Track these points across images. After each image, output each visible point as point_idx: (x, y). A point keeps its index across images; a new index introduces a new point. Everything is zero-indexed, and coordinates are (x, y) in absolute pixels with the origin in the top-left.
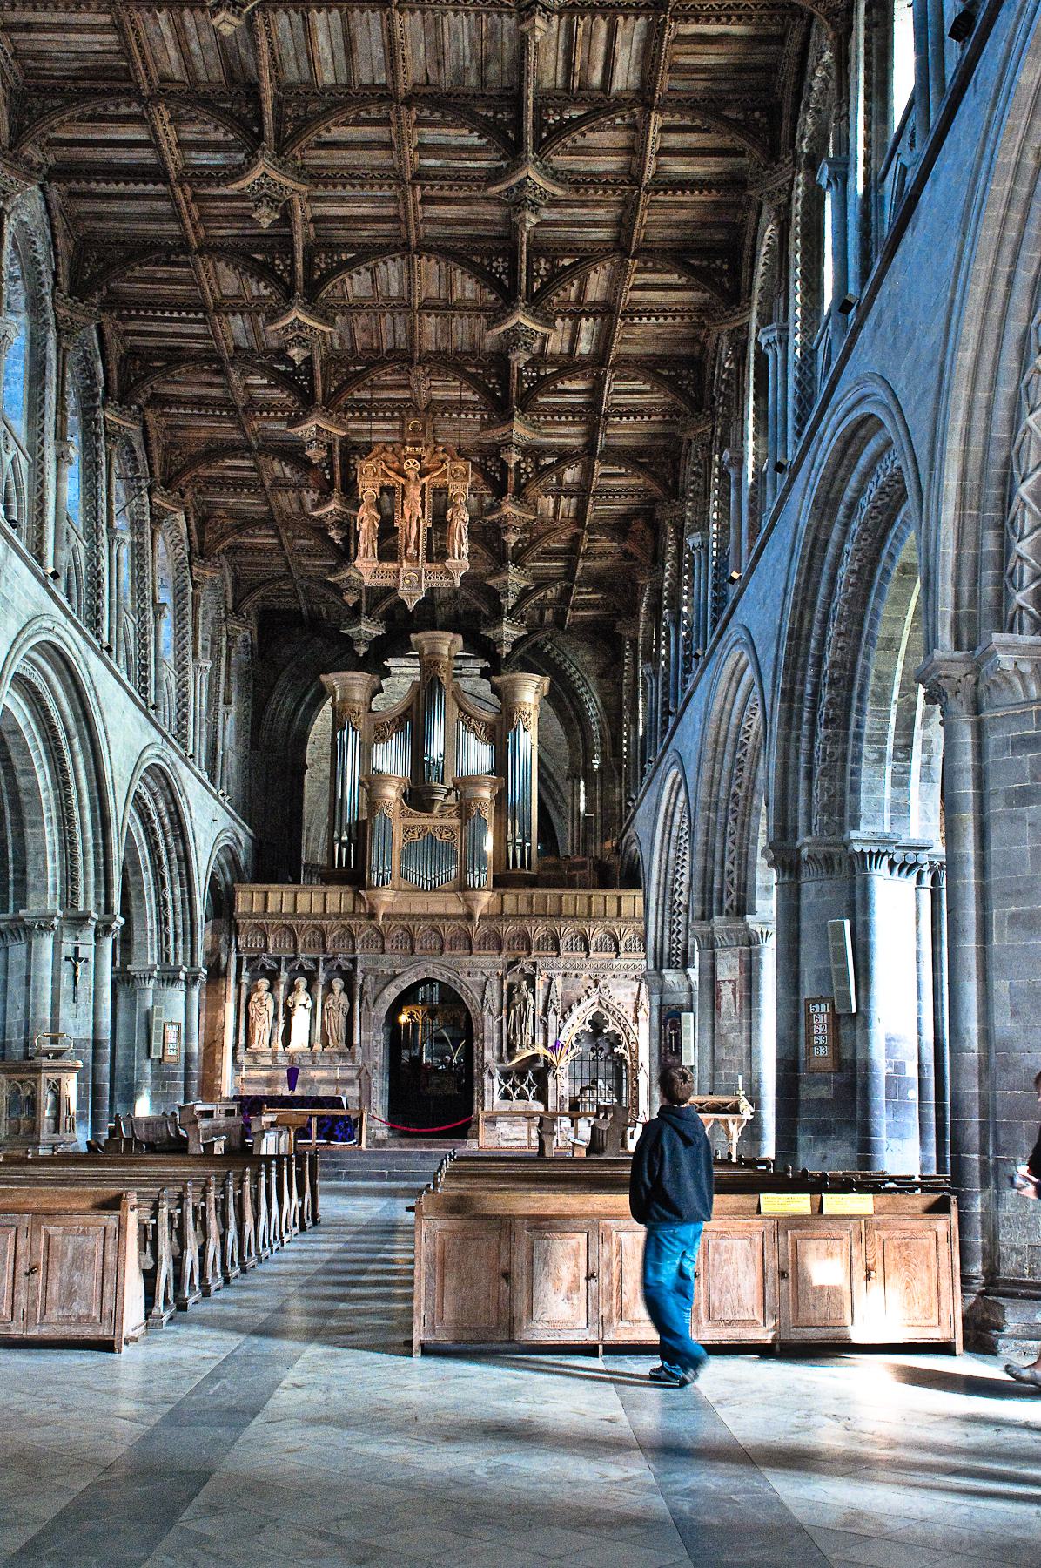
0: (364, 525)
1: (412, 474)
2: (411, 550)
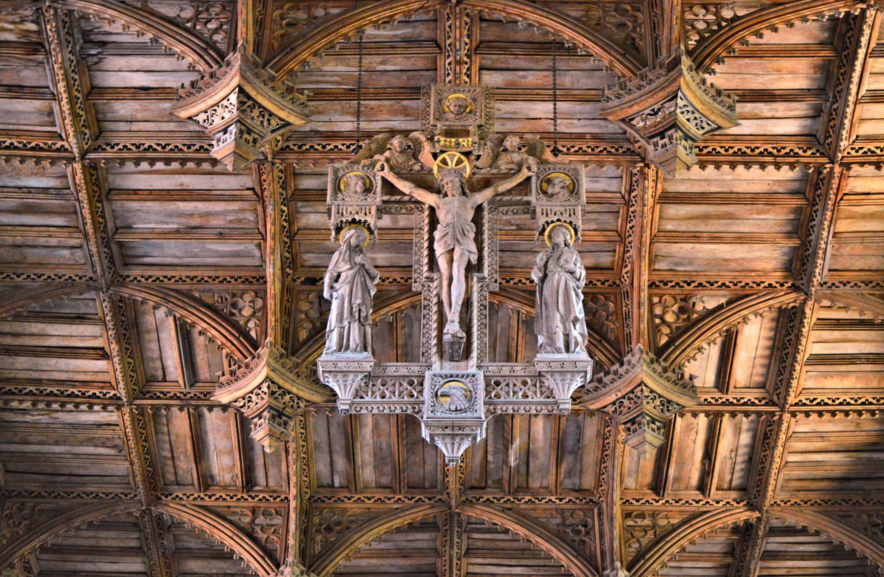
0: (343, 289)
1: (450, 184)
2: (453, 327)
